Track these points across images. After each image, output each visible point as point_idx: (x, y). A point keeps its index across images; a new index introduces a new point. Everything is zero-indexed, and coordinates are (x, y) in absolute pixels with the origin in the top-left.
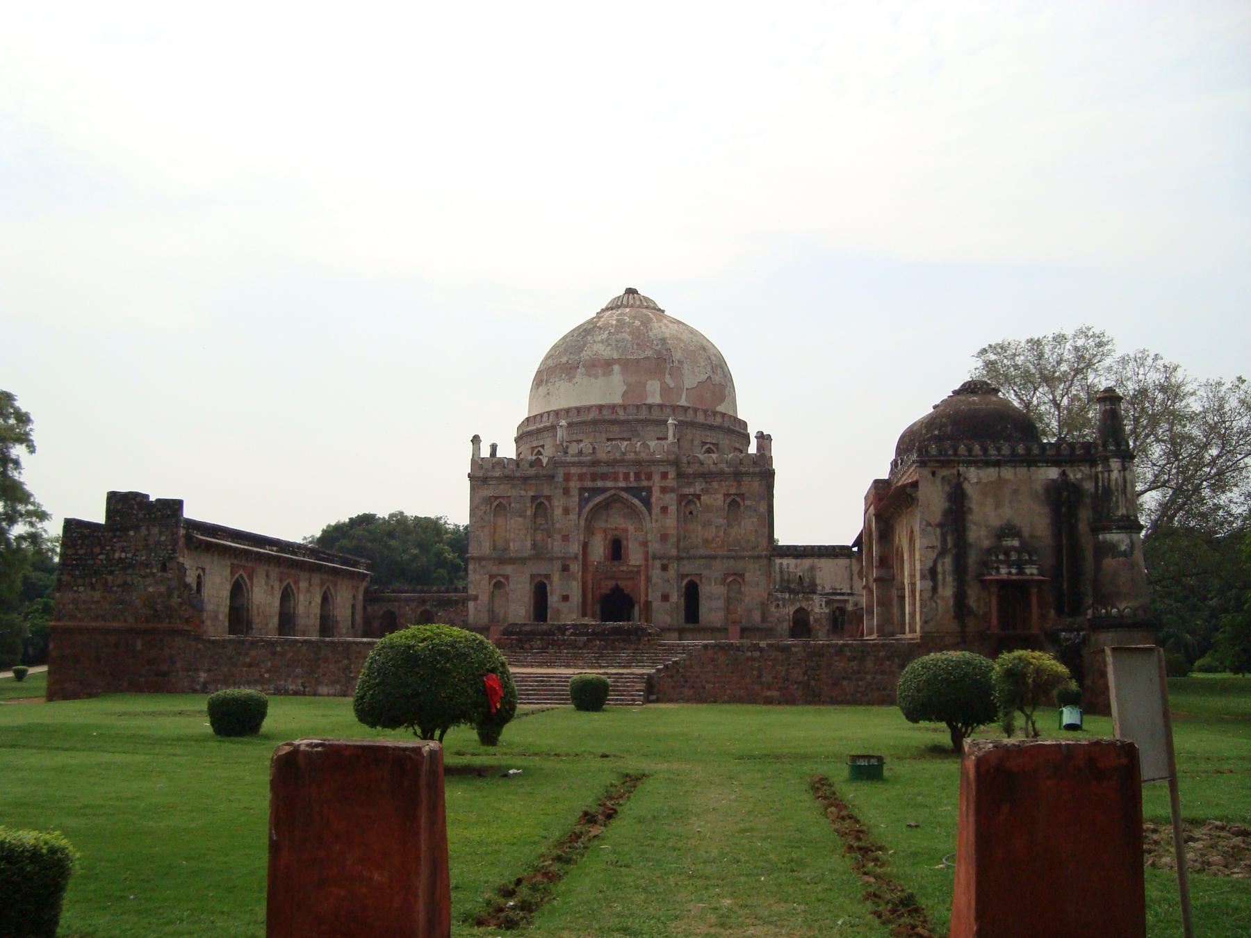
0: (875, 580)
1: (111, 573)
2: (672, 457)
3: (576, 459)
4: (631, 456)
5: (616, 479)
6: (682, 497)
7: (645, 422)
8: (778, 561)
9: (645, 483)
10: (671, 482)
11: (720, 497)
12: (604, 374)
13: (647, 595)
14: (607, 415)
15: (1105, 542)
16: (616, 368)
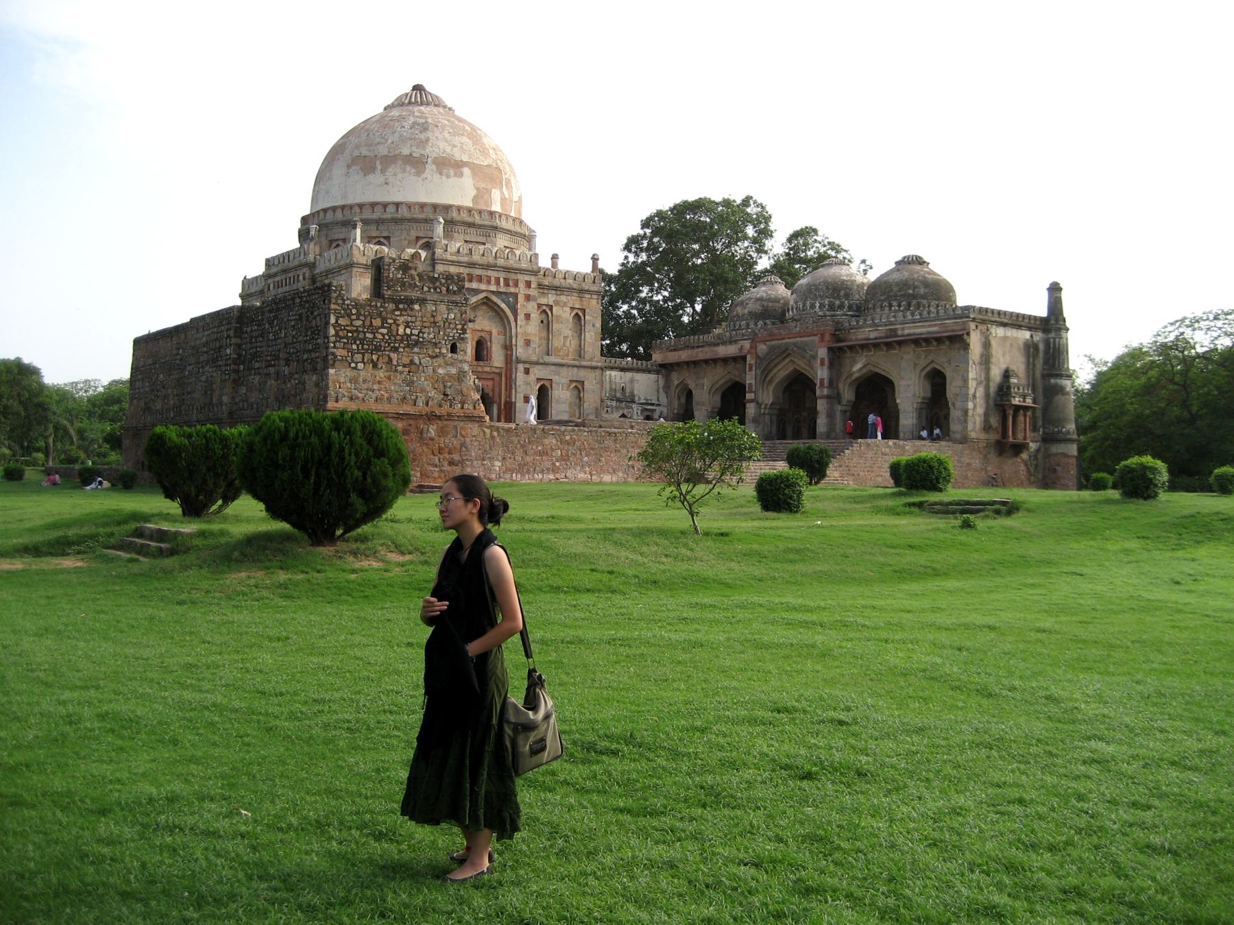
0: (828, 397)
1: (395, 350)
2: (535, 268)
3: (454, 258)
4: (501, 262)
5: (489, 282)
6: (539, 306)
7: (495, 228)
8: (608, 373)
9: (512, 290)
10: (533, 292)
11: (568, 310)
12: (455, 175)
13: (510, 396)
14: (464, 216)
15: (1056, 385)
16: (466, 171)
